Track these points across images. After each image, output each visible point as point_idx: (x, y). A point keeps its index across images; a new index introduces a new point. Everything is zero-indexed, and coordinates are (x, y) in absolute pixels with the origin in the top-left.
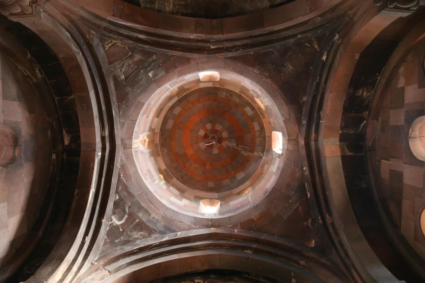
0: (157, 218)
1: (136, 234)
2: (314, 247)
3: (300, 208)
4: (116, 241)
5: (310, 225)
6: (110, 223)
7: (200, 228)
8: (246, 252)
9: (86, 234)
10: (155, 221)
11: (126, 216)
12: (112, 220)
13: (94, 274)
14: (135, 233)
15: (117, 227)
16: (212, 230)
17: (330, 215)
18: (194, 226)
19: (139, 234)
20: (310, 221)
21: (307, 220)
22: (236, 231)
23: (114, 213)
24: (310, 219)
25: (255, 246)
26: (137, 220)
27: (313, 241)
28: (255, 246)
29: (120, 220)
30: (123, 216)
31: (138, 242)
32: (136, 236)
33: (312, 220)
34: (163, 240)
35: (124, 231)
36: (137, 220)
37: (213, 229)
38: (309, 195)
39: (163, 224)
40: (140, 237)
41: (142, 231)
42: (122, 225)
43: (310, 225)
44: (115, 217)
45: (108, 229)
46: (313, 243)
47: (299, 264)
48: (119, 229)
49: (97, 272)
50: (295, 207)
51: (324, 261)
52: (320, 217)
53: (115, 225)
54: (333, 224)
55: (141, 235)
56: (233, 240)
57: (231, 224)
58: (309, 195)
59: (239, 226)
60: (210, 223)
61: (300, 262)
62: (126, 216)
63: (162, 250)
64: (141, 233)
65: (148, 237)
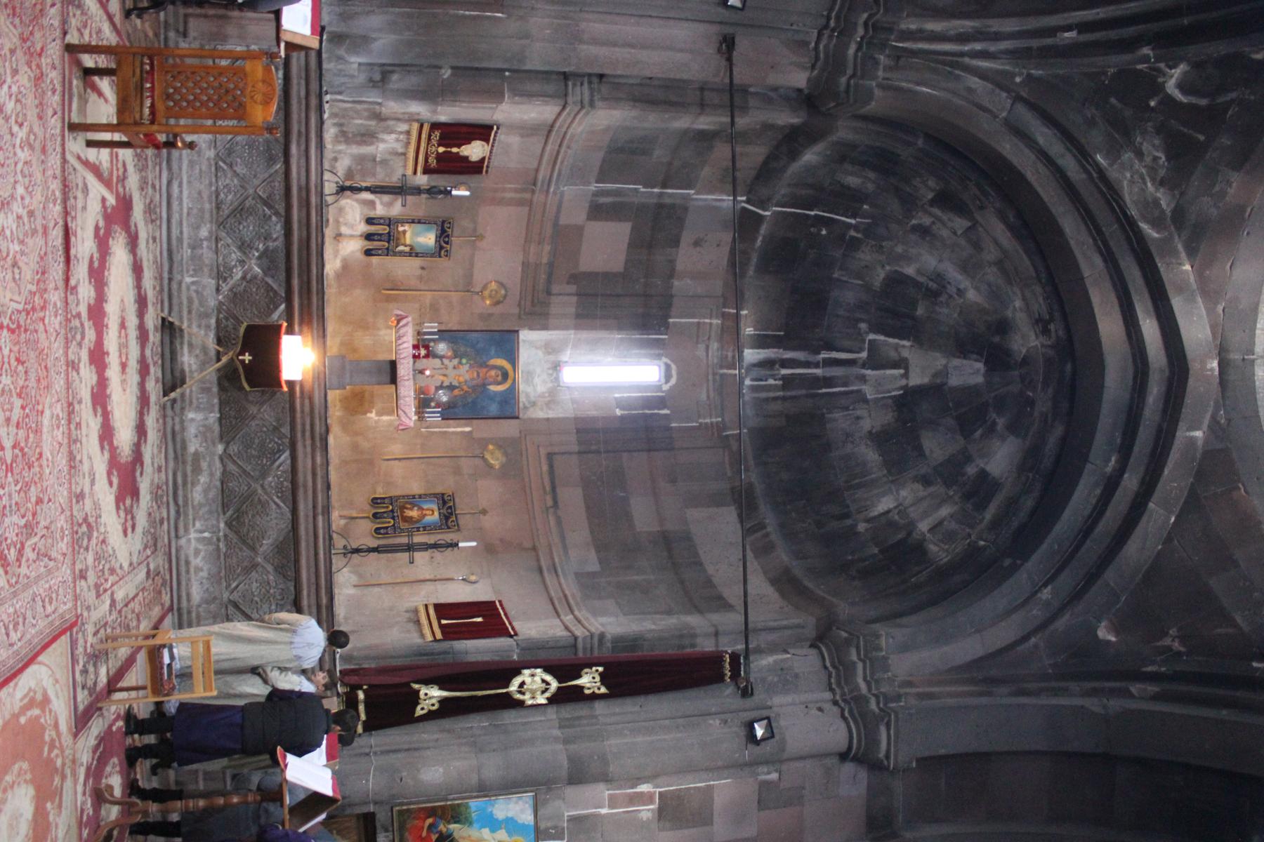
0: (1231, 191)
1: (1154, 146)
2: (1097, 636)
3: (1230, 630)
4: (1113, 100)
5: (1167, 642)
6: (1162, 65)
7: (1213, 328)
8: (1113, 459)
9: (1083, 27)
10: (1217, 188)
11: (1203, 102)
12: (1171, 68)
13: (990, 86)
14: (1157, 142)
15: (1158, 89)
16: (1203, 363)
17: (1155, 698)
18: (1220, 308)
19: (1157, 154)
20: (1176, 645)
21: (1183, 639)
22: (1198, 434)
23: (1197, 66)
24: (1182, 649)
25: (1131, 482)
26: (1202, 138)
27: (1113, 639)
28: (1131, 482)
29: (1181, 86)
30: (1203, 96)
31: (1128, 156)
32: (1146, 147)
33: (1179, 654)
34: (1144, 226)
35: (1153, 109)
36: (1202, 138)
37: (1215, 364)
38: (1255, 664)
39: (1214, 212)
40: (1148, 159)
41: (1168, 159)
42: (1169, 100)
43: (1167, 642)
44: (1185, 73)
45: (1139, 67)
46: (1104, 633)
47: (1045, 585)
48: (1151, 98)
49: (997, 91)
50: (1239, 620)
51: (1033, 640)
52: (1163, 669)
53: (1160, 80)
54: (1128, 694)
55: (1156, 159)
56: (1165, 426)
57: (1229, 421)
58: (1255, 664)
59: (1220, 446)
60: (1235, 356)
61: (1049, 587)
62: (1203, 102)
63: (1111, 229)
64: (1164, 158)
65: (1153, 180)
